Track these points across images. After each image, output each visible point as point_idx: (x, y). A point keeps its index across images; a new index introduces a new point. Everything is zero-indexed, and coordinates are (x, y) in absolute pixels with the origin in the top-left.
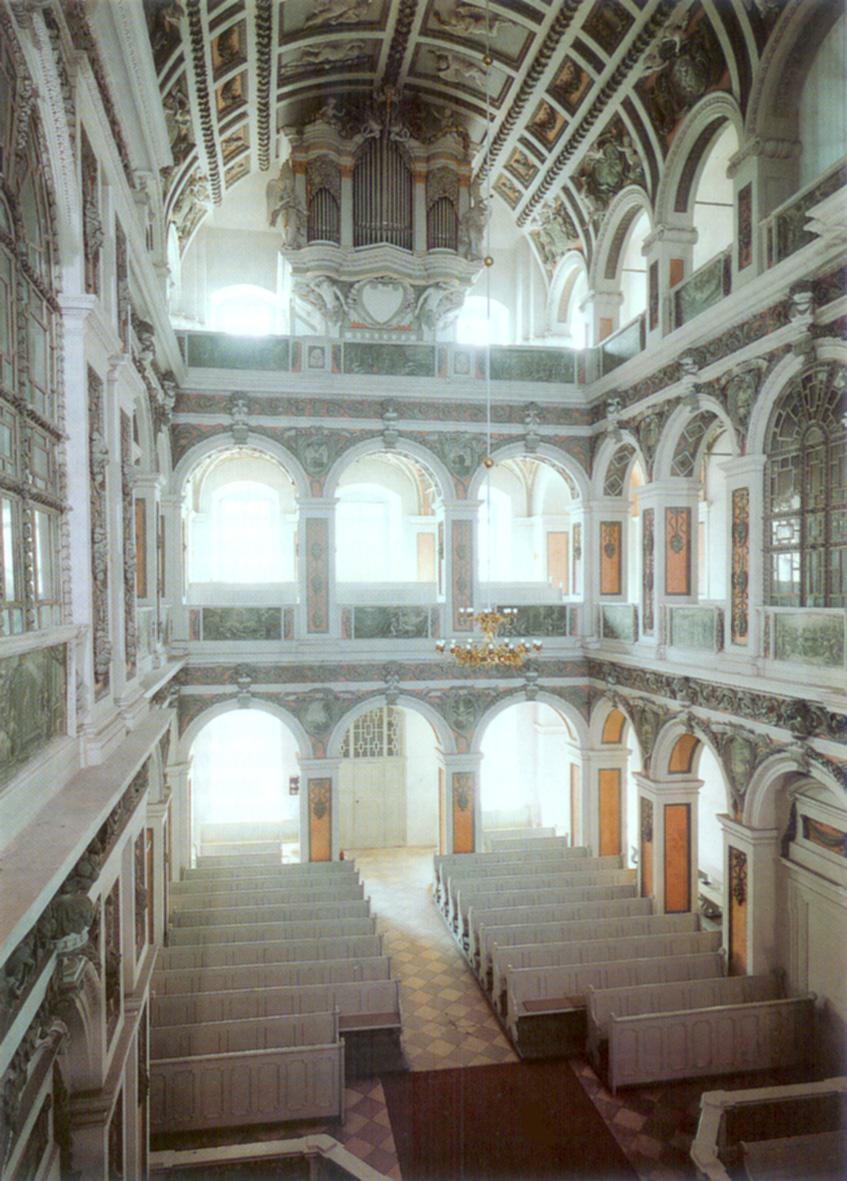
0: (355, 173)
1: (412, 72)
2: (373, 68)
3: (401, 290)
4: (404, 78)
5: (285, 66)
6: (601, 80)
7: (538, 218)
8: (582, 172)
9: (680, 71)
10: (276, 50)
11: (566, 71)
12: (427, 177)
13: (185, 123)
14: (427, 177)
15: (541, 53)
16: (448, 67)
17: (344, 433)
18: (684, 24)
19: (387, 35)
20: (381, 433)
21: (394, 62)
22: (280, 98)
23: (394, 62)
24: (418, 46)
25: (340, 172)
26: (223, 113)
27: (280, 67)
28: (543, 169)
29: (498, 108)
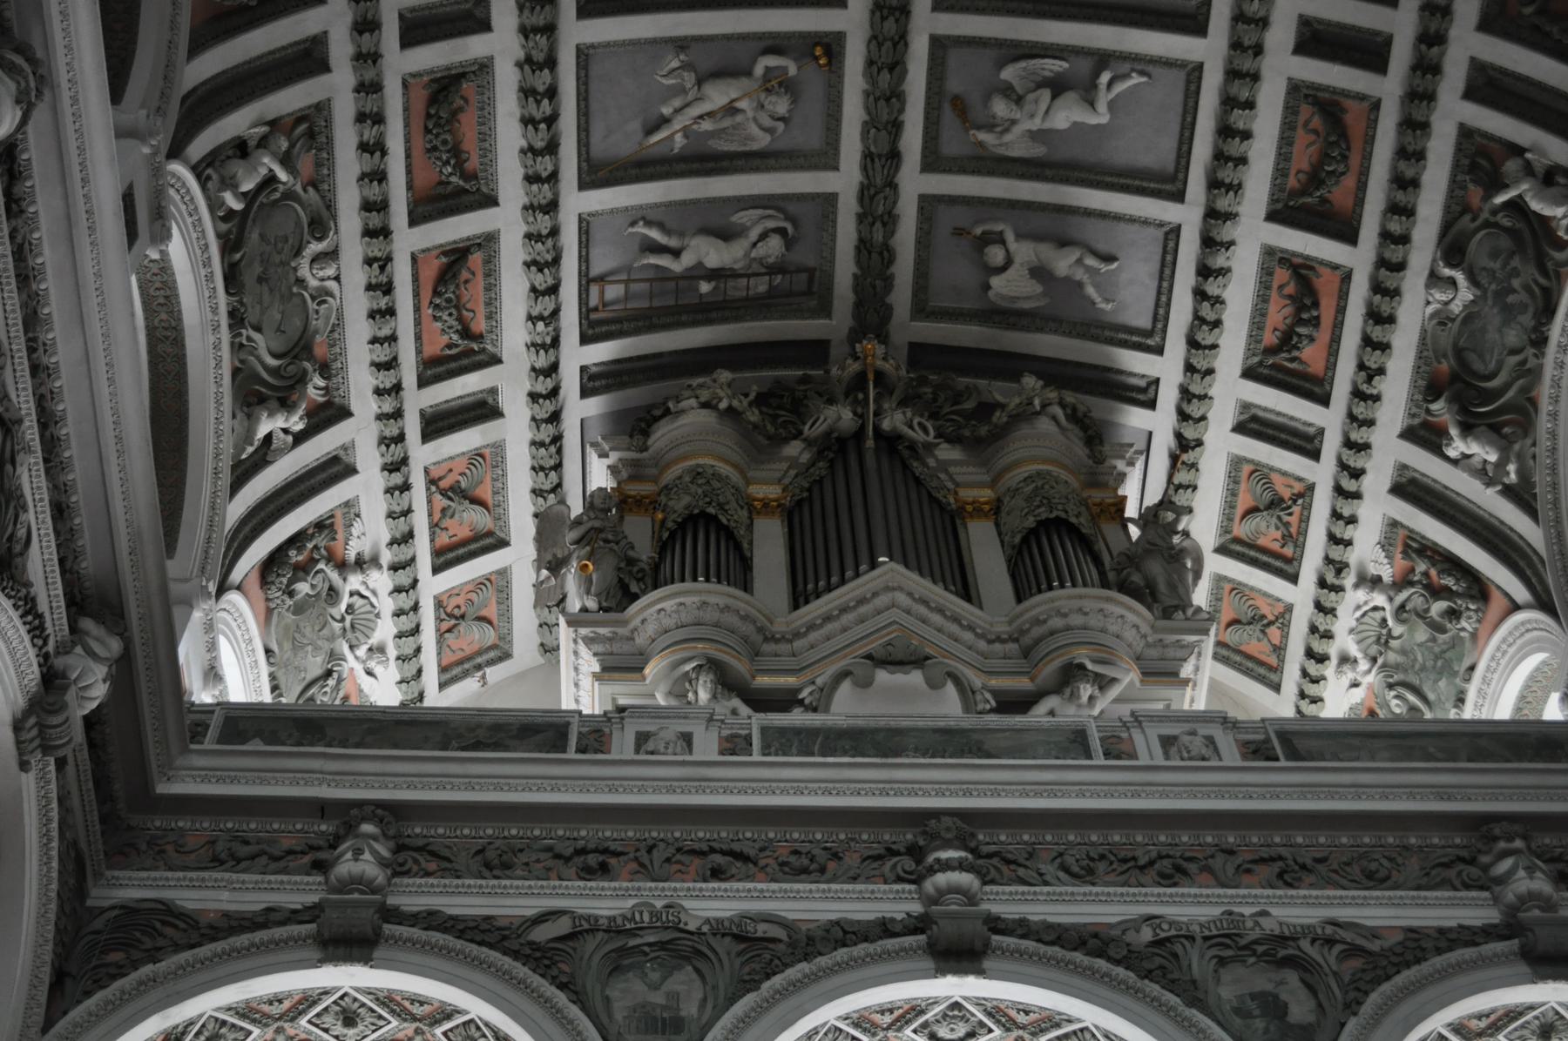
0: (793, 514)
1: (921, 309)
2: (825, 310)
3: (950, 688)
4: (907, 327)
5: (601, 279)
6: (1389, 87)
7: (1354, 650)
8: (1430, 387)
10: (576, 202)
11: (1301, 137)
12: (995, 510)
13: (322, 295)
14: (995, 510)
15: (1229, 102)
16: (1009, 262)
17: (762, 929)
19: (844, 181)
20: (917, 925)
22: (593, 382)
24: (928, 204)
25: (755, 509)
26: (434, 370)
27: (586, 281)
28: (1322, 474)
29: (1159, 350)
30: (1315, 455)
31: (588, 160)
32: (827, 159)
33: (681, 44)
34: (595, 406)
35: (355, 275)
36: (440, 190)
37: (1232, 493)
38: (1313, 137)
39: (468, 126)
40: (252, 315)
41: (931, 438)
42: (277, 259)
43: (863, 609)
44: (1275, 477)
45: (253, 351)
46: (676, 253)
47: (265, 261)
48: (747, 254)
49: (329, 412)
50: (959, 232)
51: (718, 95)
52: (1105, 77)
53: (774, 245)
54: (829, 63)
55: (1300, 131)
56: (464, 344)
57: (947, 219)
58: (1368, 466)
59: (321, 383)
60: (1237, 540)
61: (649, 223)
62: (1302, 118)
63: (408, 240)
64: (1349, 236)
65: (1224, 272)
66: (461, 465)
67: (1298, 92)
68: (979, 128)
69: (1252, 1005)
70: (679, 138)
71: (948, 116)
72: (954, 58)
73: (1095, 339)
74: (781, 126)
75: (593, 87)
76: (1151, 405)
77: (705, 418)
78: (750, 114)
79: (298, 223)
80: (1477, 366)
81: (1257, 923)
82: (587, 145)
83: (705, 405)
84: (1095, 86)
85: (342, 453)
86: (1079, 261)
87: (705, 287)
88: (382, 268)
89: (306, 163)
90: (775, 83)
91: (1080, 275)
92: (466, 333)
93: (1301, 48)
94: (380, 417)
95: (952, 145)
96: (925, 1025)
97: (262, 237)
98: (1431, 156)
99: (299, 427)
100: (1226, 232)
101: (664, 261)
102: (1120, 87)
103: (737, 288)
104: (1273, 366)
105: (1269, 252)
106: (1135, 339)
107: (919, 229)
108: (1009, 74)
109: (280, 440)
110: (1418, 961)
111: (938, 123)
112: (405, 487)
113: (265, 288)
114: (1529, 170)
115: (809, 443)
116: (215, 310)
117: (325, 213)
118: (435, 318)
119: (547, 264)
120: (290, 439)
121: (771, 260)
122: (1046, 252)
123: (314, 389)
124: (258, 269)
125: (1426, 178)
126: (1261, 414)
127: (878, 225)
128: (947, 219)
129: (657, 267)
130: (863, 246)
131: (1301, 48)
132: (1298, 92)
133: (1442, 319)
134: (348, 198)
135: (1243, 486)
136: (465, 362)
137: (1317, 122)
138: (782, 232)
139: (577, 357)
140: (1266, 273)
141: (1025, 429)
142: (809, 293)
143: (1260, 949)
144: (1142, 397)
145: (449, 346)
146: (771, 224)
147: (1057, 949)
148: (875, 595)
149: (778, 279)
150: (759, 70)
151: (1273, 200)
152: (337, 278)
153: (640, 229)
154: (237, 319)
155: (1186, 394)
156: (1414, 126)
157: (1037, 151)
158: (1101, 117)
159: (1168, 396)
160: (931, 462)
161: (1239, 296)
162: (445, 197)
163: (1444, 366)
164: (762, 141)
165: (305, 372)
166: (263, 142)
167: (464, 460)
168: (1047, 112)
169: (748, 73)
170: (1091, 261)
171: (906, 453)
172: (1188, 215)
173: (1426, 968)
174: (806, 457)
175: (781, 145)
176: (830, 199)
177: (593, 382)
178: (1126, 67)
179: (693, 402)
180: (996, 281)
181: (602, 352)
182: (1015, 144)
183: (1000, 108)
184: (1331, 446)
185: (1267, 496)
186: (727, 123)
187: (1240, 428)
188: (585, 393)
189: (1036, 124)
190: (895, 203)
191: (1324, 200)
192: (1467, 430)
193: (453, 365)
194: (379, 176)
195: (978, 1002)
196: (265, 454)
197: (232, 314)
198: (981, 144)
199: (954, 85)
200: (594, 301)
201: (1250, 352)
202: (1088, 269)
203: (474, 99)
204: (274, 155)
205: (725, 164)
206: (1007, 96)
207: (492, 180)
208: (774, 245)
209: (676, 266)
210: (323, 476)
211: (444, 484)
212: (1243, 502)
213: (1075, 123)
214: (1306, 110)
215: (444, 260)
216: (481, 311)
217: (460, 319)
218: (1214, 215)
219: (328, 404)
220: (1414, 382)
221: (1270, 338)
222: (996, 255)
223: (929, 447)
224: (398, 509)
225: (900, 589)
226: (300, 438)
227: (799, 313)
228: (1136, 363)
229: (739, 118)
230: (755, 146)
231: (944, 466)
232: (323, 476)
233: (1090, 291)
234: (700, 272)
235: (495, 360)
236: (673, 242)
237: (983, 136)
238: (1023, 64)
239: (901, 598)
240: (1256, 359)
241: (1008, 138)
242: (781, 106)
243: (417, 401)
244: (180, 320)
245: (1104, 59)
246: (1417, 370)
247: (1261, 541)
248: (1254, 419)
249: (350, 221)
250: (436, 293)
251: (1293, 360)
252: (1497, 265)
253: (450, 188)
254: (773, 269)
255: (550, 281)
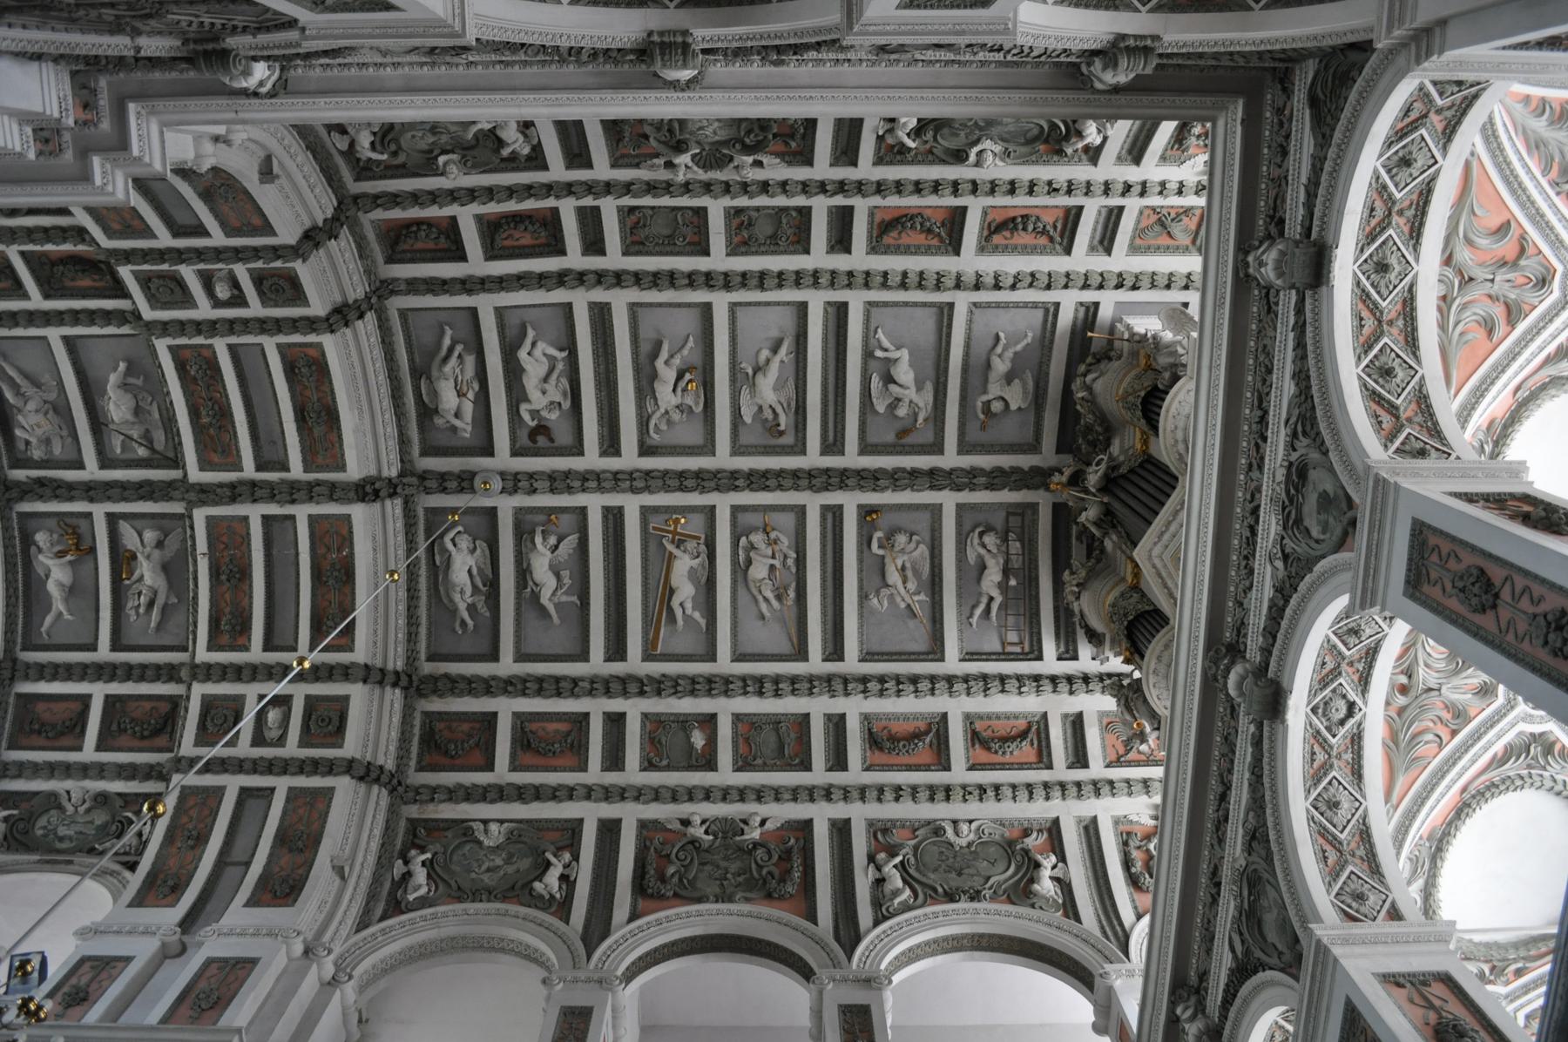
1: (1034, 447)
2: (1034, 507)
4: (1047, 456)
9: (715, 133)
10: (952, 663)
18: (660, 161)
19: (948, 500)
21: (996, 479)
22: (1070, 654)
23: (996, 479)
24: (964, 448)
26: (1044, 759)
27: (1004, 656)
28: (1133, 204)
30: (1121, 209)
31: (928, 653)
32: (936, 511)
33: (863, 597)
34: (1085, 650)
35: (973, 809)
36: (935, 747)
37: (1158, 250)
38: (903, 235)
39: (899, 728)
40: (977, 883)
41: (1106, 458)
42: (951, 860)
43: (1164, 574)
44: (1142, 225)
45: (1000, 884)
46: (991, 599)
47: (950, 869)
48: (994, 556)
49: (1054, 832)
50: (983, 427)
51: (894, 577)
52: (879, 353)
53: (990, 540)
54: (876, 512)
55: (901, 242)
56: (1032, 735)
57: (974, 434)
58: (1122, 180)
59: (1034, 835)
60: (1194, 242)
61: (971, 615)
62: (891, 241)
63: (959, 773)
64: (962, 212)
65: (997, 277)
66: (1111, 738)
67: (875, 248)
68: (916, 421)
69: (1323, 517)
70: (922, 597)
71: (909, 440)
72: (872, 438)
73: (1052, 342)
74: (915, 538)
75: (886, 649)
76: (1097, 305)
77: (1085, 597)
78: (906, 558)
79: (934, 843)
80: (1036, 131)
81: (1279, 483)
82: (919, 653)
83: (1078, 598)
84: (887, 360)
85: (1083, 824)
86: (1000, 356)
87: (1013, 582)
88: (970, 793)
89: (897, 836)
90: (888, 542)
91: (1009, 354)
92: (1023, 735)
93: (847, 250)
94: (1064, 797)
95: (928, 437)
96: (1328, 729)
97: (935, 870)
98: (898, 177)
99: (1053, 859)
100: (969, 278)
101: (995, 607)
102: (886, 343)
103: (1016, 563)
104: (1062, 236)
105: (981, 250)
106: (1050, 318)
107: (980, 453)
108: (881, 408)
109: (1058, 873)
110: (1308, 377)
111: (913, 446)
112: (1111, 783)
113: (966, 871)
114: (890, 131)
115: (1106, 534)
116: (965, 912)
117: (932, 826)
118: (1011, 753)
119: (986, 684)
120: (1060, 865)
121: (998, 542)
122: (993, 376)
123: (1033, 842)
124: (953, 875)
125: (914, 177)
126: (1098, 237)
127: (975, 481)
128: (974, 434)
129: (999, 608)
130: (990, 487)
131: (847, 250)
132: (875, 248)
133: (1007, 154)
134: (925, 811)
135: (1152, 242)
136: (1043, 735)
137: (894, 234)
138: (981, 534)
139: (1050, 663)
140: (996, 250)
141: (1101, 400)
142: (1022, 515)
143: (1292, 491)
144: (1092, 310)
145: (1032, 744)
146: (976, 541)
147: (1279, 635)
148: (1154, 566)
149: (1012, 536)
150: (881, 552)
151: (947, 253)
152: (971, 822)
153: (974, 620)
154: (975, 896)
155: (1085, 286)
156: (880, 188)
157: (929, 387)
158: (904, 354)
159: (1089, 296)
160: (1122, 458)
161: (1011, 264)
162: (939, 744)
163: (1042, 147)
164: (923, 550)
165: (1023, 849)
166: (879, 869)
167: (1107, 736)
168: (901, 386)
169: (883, 557)
170: (999, 350)
171: (1115, 474)
172: (962, 301)
173: (1313, 373)
174: (1114, 537)
175: (927, 538)
176: (960, 508)
177: (1070, 654)
178: (873, 342)
179: (1076, 604)
180: (1013, 407)
181: (1049, 647)
182: (925, 400)
183: (902, 412)
184: (1115, 201)
185: (1157, 228)
186: (909, 573)
187: (1108, 251)
188: (1075, 658)
189: (914, 389)
190: (962, 470)
191: (943, 224)
192: (1080, 135)
193: (1044, 744)
194: (914, 790)
195: (1313, 693)
196: (1064, 885)
197: (972, 899)
198: (925, 420)
199: (890, 437)
200: (1018, 649)
201: (1053, 252)
202: (1004, 350)
203: (884, 723)
204: (887, 862)
205: (937, 570)
206: (896, 407)
207: (932, 715)
208: (990, 540)
209: (998, 599)
210: (1093, 840)
211: (1121, 751)
212: (1167, 241)
213: (910, 366)
214: (887, 240)
215: (977, 746)
216: (1013, 722)
217: (1013, 739)
218: (958, 285)
219: (1049, 831)
220: (1055, 163)
221: (1043, 240)
222: (997, 407)
223: (1111, 458)
224: (1126, 790)
225: (1150, 551)
226: (1062, 858)
227: (1035, 522)
228: (1066, 318)
229: (908, 565)
230: (927, 554)
231: (1123, 451)
232: (1093, 840)
233: (1019, 347)
234: (1003, 586)
235: (1045, 715)
236: (985, 600)
237: (920, 420)
238: (874, 400)
239: (1156, 552)
240: (1058, 247)
241: (921, 405)
242: (901, 539)
243: (1061, 770)
244: (967, 934)
245: (868, 354)
246: (1046, 163)
247: (1193, 227)
248: (1101, 242)
249: (939, 811)
250: (996, 752)
251: (1055, 227)
252: (962, 134)
253: (935, 741)
254: (1005, 540)
255: (997, 683)
